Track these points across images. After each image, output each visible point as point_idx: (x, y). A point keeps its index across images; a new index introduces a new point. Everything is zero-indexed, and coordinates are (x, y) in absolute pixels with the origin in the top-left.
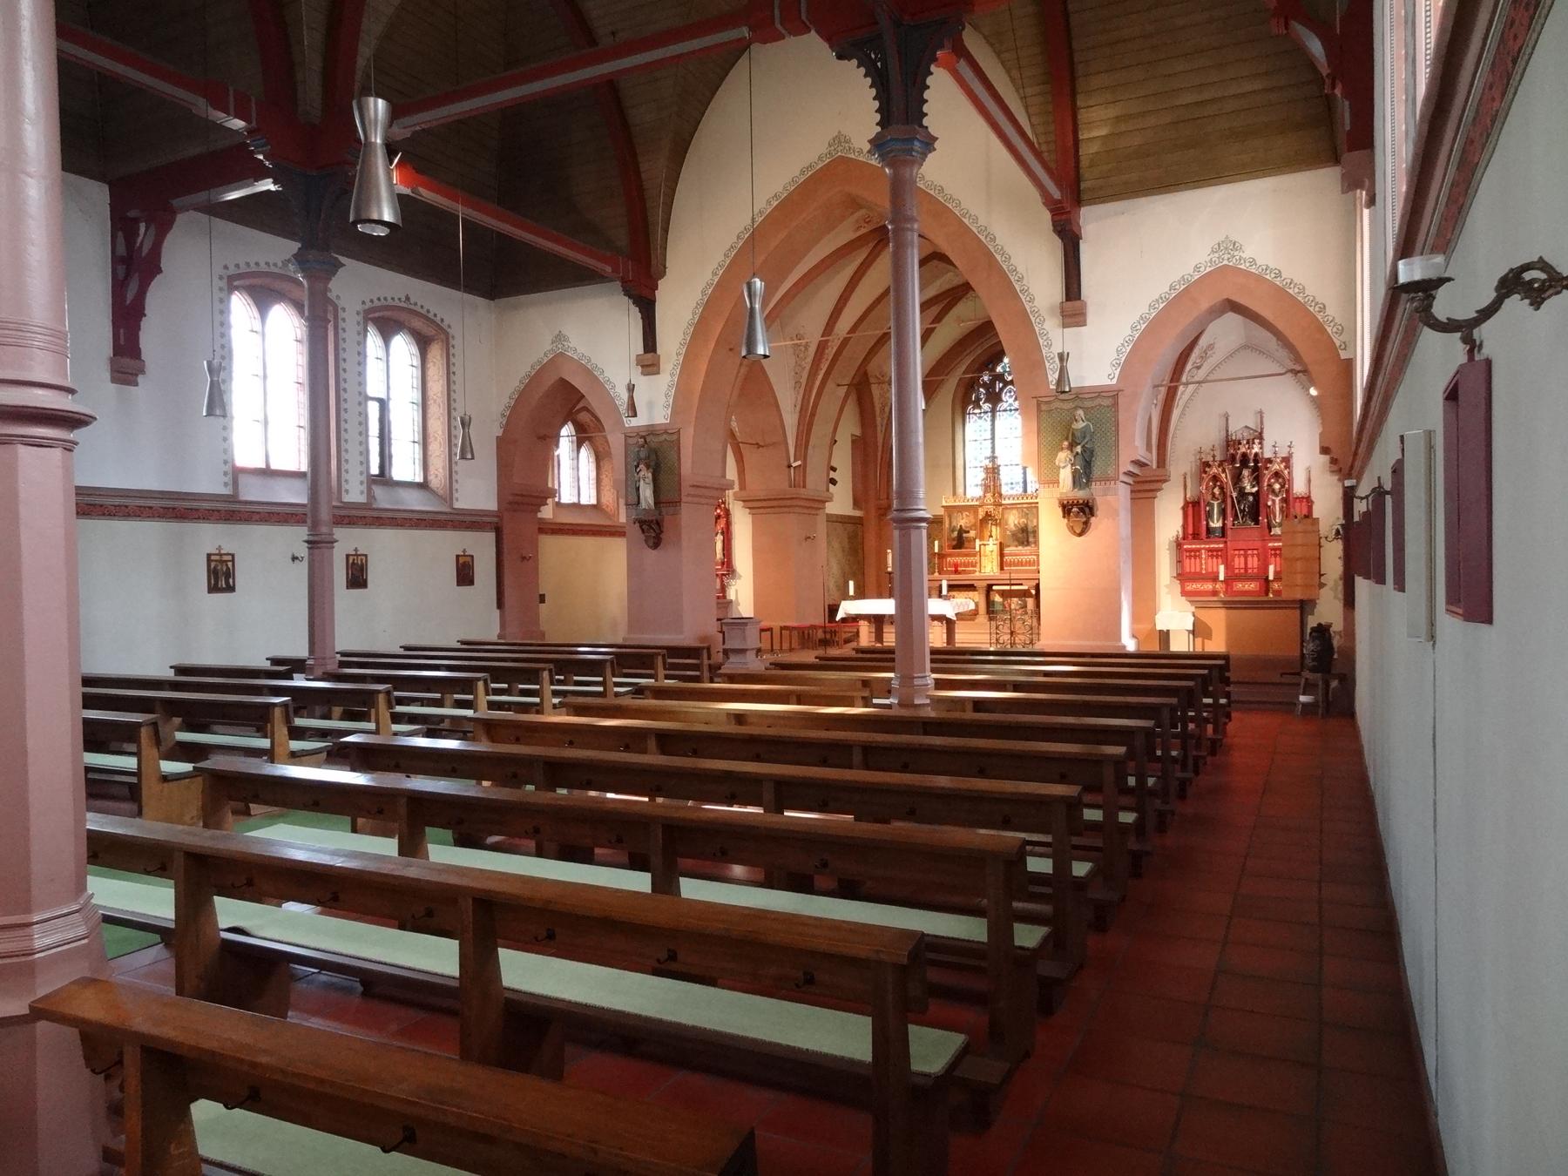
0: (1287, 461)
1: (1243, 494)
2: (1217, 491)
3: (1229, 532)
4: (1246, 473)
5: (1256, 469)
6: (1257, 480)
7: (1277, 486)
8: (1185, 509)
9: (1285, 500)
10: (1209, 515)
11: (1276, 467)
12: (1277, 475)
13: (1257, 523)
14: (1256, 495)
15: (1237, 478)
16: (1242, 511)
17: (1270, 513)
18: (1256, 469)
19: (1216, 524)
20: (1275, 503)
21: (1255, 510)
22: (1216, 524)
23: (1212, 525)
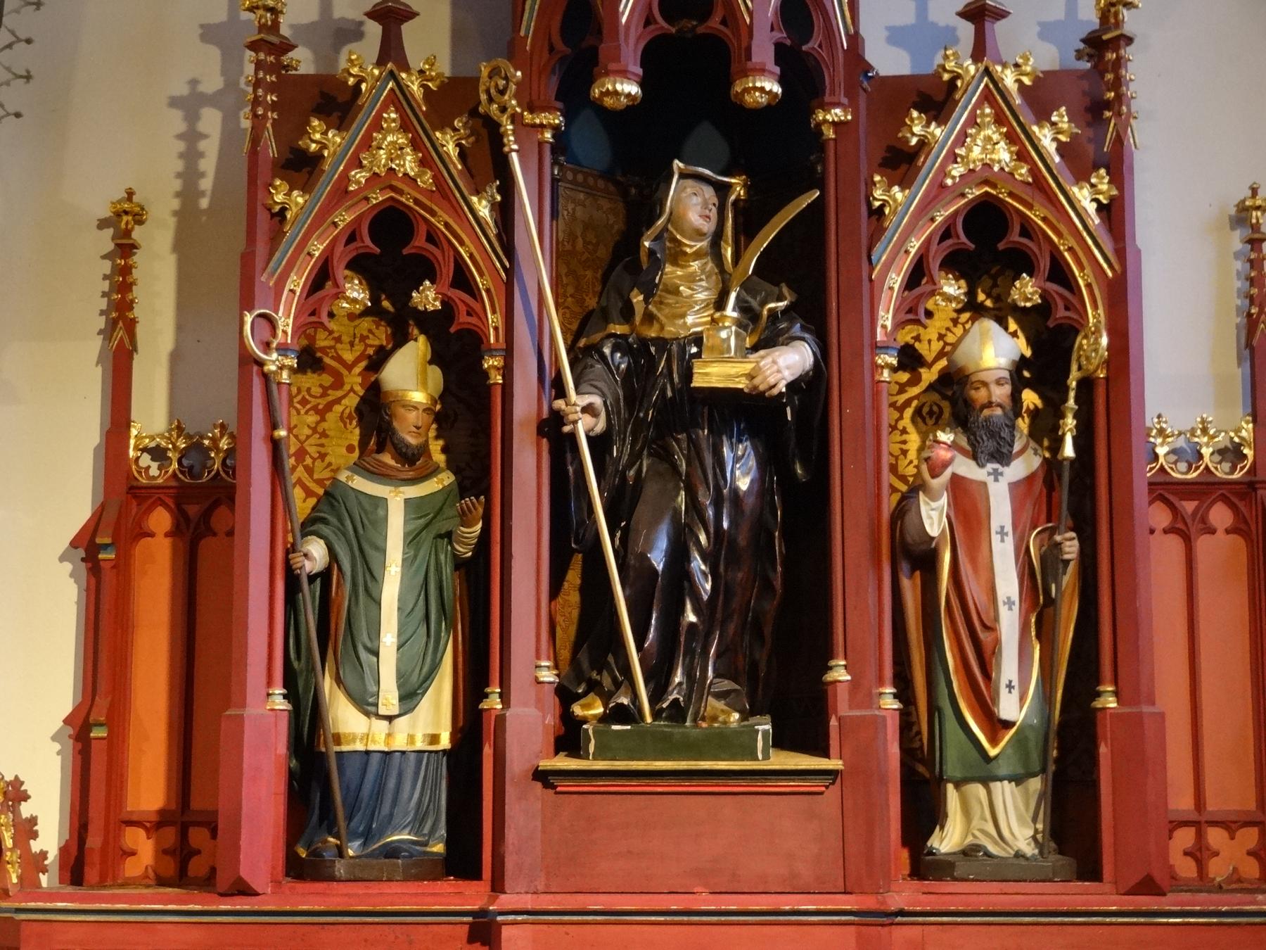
0: (1094, 84)
1: (667, 411)
2: (411, 378)
3: (525, 819)
4: (691, 204)
5: (777, 158)
6: (801, 279)
7: (995, 350)
8: (101, 555)
9: (1078, 497)
10: (324, 625)
11: (980, 150)
12: (988, 245)
13: (803, 724)
14: (794, 430)
15: (613, 269)
16: (661, 592)
17: (934, 637)
18: (777, 158)
19: (394, 719)
20: (986, 517)
21: (757, 592)
22: (394, 719)
23: (350, 724)
